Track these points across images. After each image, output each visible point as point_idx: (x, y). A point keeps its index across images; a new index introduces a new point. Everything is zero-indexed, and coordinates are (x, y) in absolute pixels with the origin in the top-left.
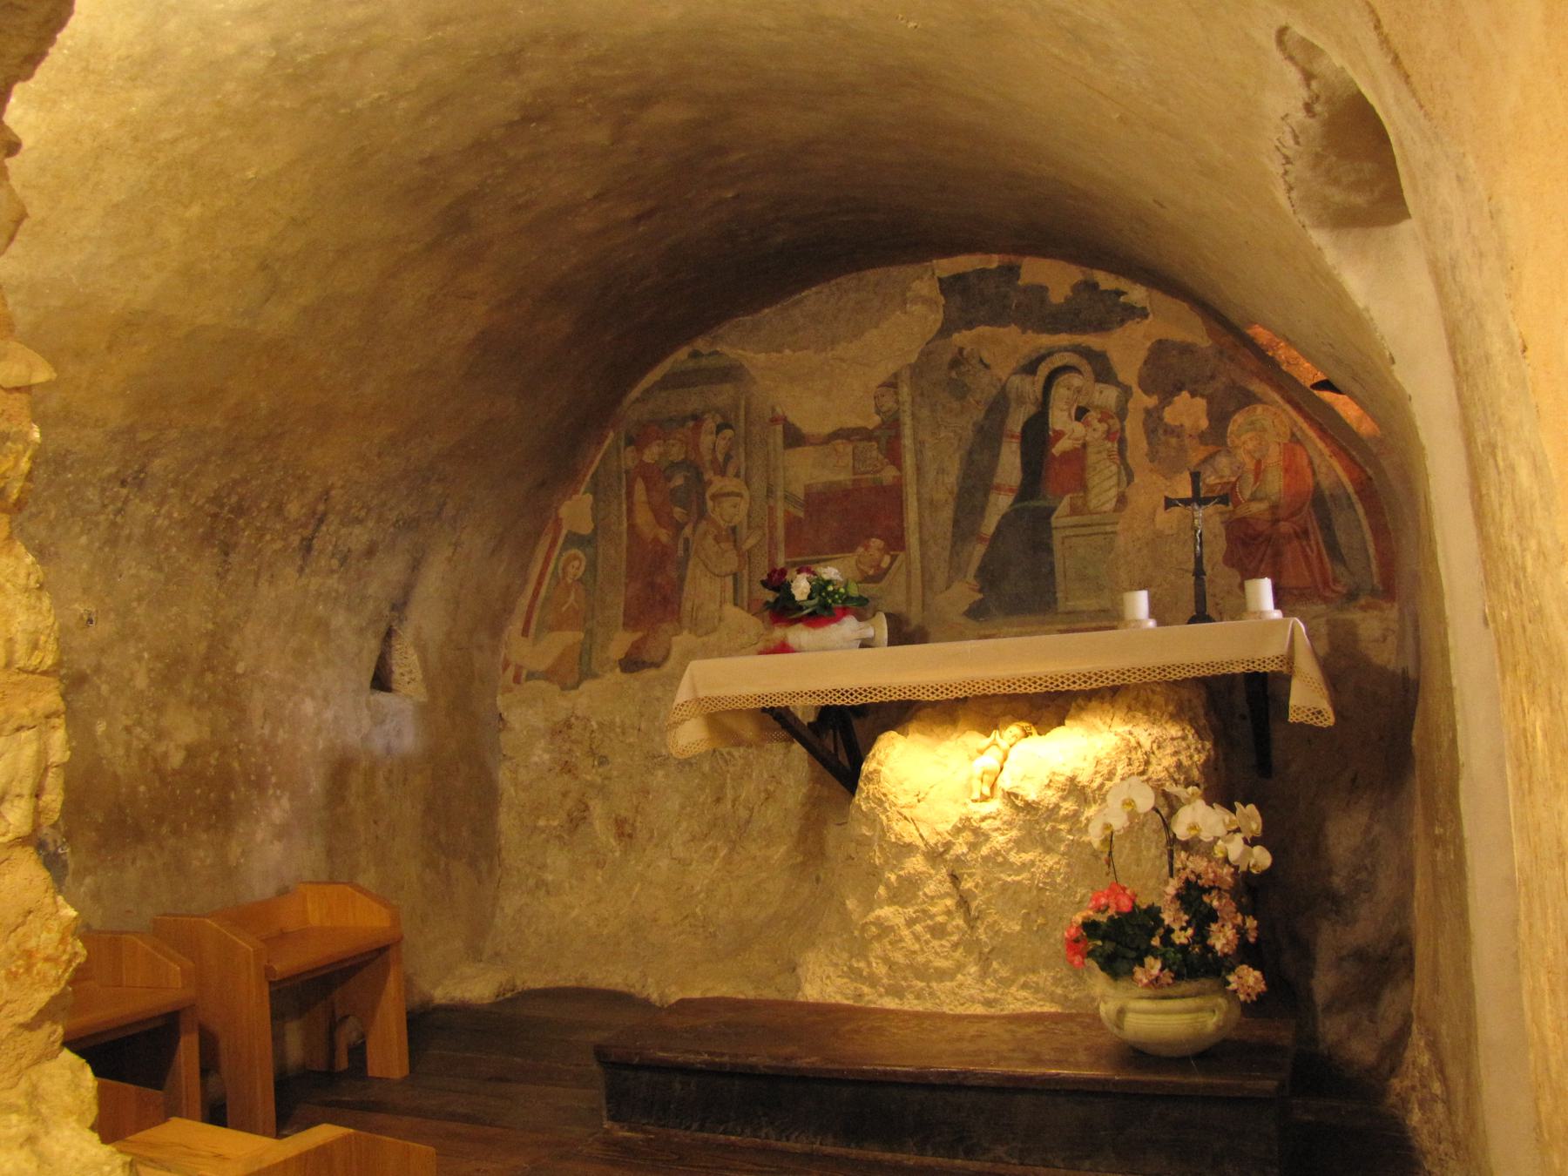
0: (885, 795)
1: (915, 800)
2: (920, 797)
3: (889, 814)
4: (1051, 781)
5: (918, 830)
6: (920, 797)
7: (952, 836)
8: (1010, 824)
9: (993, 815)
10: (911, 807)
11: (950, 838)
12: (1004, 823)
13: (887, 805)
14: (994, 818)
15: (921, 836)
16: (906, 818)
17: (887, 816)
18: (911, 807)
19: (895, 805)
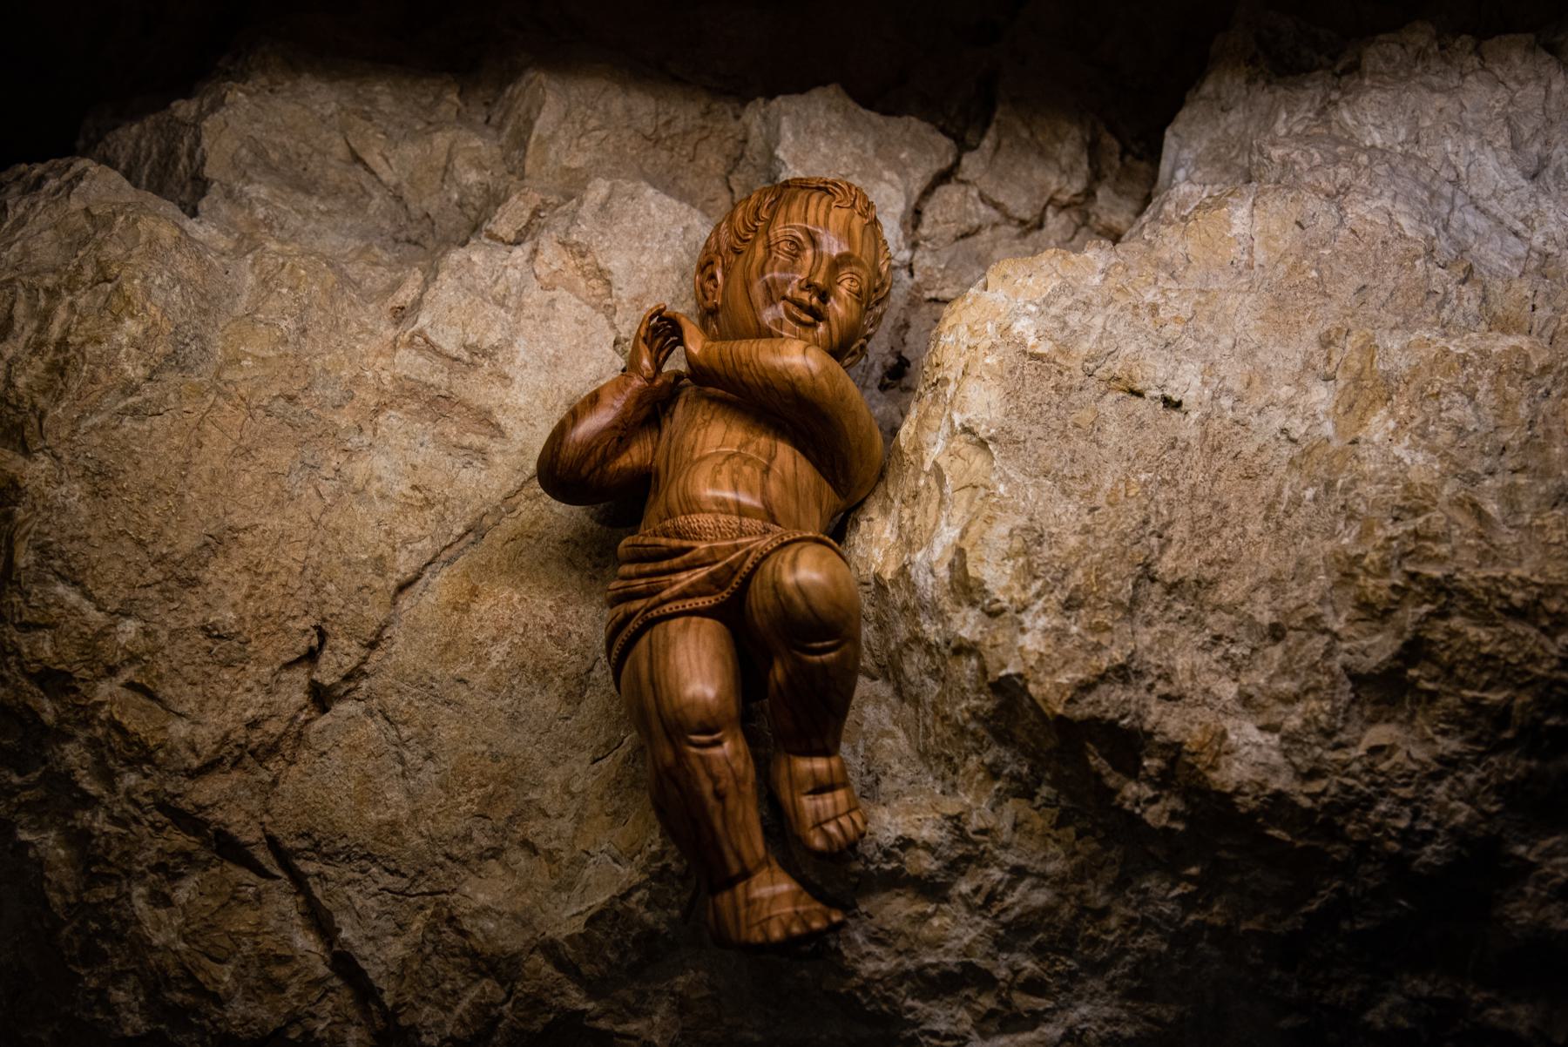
0: (55, 681)
1: (294, 693)
2: (327, 673)
3: (100, 823)
4: (1415, 650)
5: (320, 922)
6: (327, 673)
7: (592, 989)
8: (1066, 941)
9: (927, 864)
10: (273, 750)
11: (576, 999)
12: (1013, 934)
13: (73, 754)
14: (932, 889)
15: (345, 964)
16: (228, 848)
17: (80, 839)
18: (273, 750)
19: (141, 755)
